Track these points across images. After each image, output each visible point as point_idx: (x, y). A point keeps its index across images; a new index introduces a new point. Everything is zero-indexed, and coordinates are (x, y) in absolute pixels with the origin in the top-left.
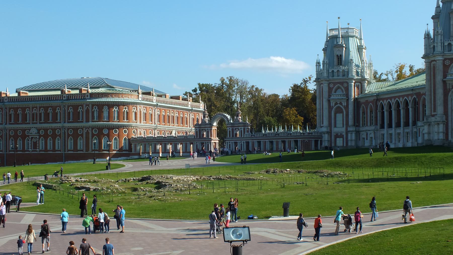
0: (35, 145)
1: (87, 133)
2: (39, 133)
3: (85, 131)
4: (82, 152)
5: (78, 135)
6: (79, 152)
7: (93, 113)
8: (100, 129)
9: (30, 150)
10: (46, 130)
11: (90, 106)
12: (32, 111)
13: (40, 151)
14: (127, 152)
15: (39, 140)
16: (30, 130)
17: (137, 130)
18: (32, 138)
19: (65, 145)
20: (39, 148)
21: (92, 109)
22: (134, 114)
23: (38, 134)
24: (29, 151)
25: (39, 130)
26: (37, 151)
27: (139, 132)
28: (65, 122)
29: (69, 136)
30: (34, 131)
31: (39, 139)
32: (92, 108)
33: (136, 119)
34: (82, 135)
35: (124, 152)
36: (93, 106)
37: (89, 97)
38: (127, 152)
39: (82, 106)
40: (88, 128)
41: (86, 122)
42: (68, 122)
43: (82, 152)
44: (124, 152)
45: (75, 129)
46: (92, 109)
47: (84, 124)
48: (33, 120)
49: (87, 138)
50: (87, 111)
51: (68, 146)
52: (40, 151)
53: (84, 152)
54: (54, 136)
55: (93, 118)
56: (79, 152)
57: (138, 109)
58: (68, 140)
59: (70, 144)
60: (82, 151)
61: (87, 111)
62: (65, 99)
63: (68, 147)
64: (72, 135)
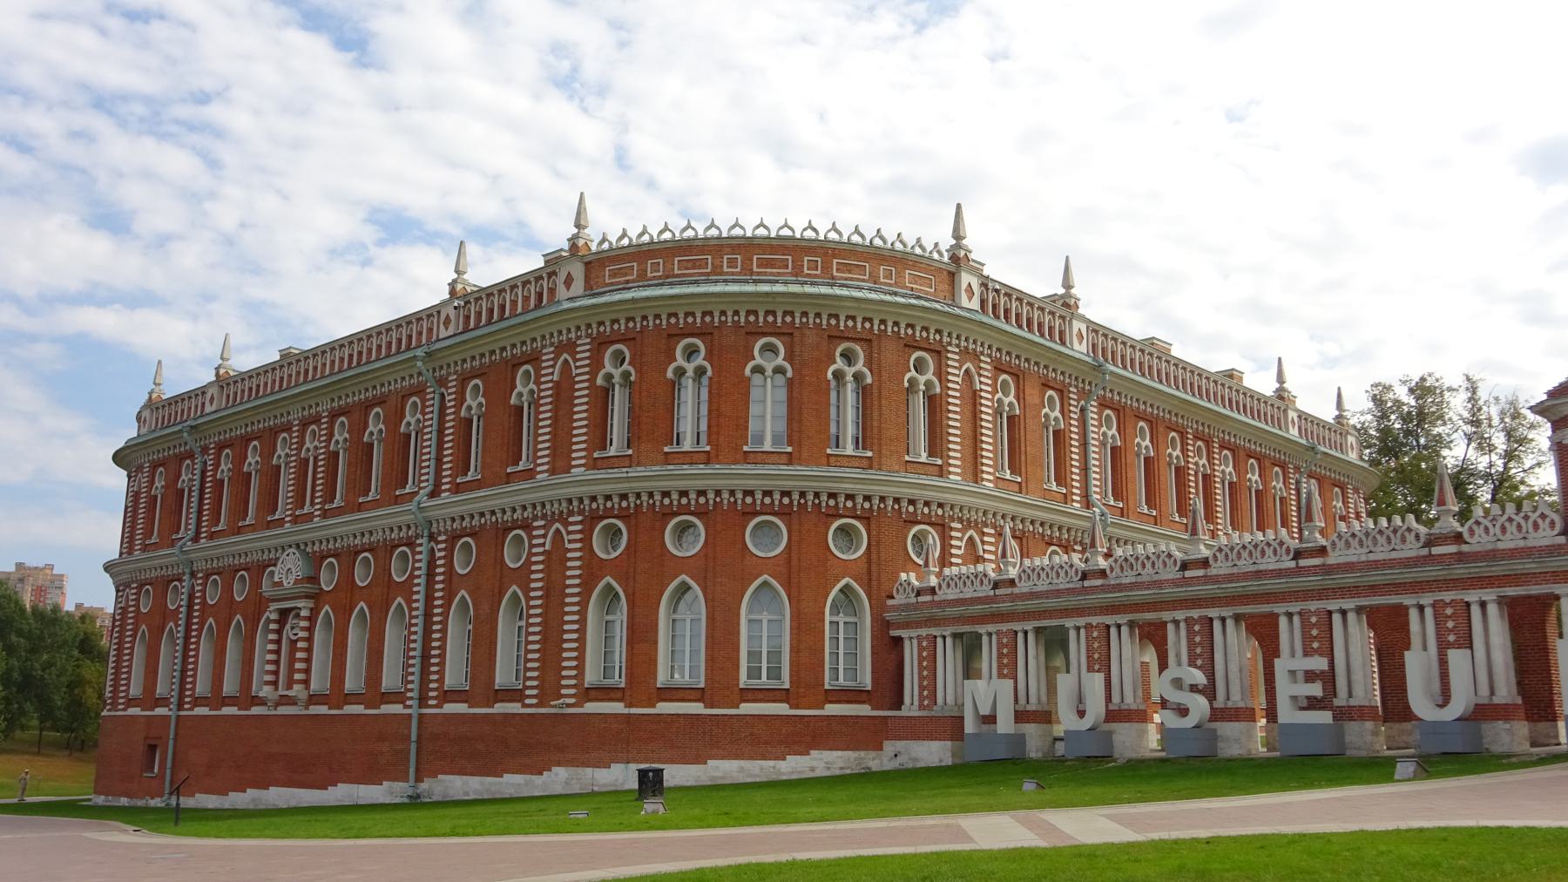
0: (292, 661)
2: (314, 579)
4: (514, 708)
5: (503, 577)
7: (602, 398)
8: (644, 518)
9: (266, 692)
10: (348, 556)
11: (584, 346)
13: (314, 699)
14: (864, 710)
15: (310, 629)
17: (943, 528)
18: (284, 614)
20: (306, 682)
21: (593, 374)
22: (919, 404)
23: (308, 588)
24: (261, 702)
25: (316, 560)
27: (959, 546)
28: (434, 494)
30: (289, 570)
31: (312, 619)
32: (596, 364)
33: (936, 444)
34: (522, 576)
35: (832, 709)
36: (600, 344)
37: (578, 287)
38: (864, 710)
39: (534, 359)
41: (553, 472)
43: (514, 708)
44: (832, 709)
45: (492, 534)
46: (593, 374)
47: (545, 487)
49: (553, 594)
50: (563, 392)
51: (442, 664)
52: (314, 699)
55: (600, 438)
57: (956, 377)
58: (447, 606)
61: (563, 392)
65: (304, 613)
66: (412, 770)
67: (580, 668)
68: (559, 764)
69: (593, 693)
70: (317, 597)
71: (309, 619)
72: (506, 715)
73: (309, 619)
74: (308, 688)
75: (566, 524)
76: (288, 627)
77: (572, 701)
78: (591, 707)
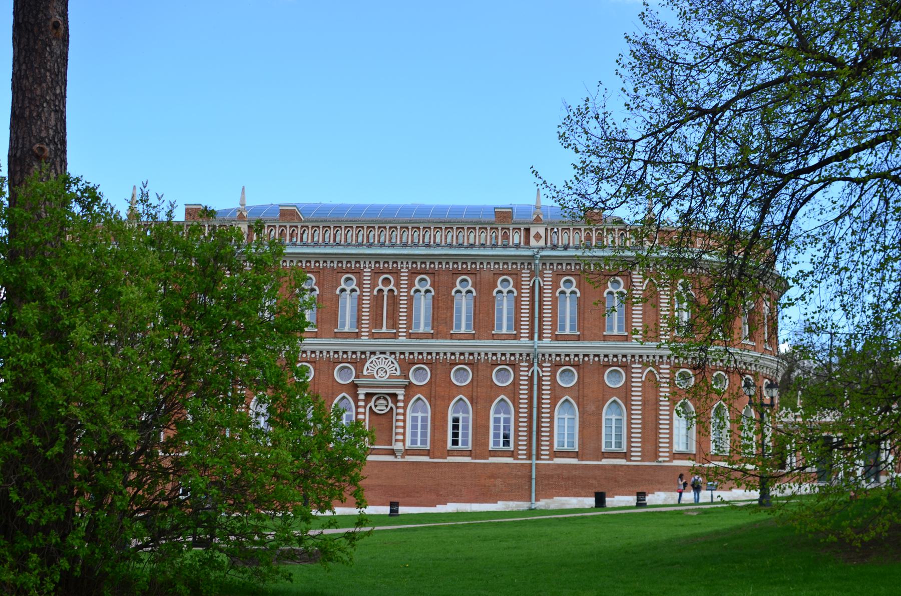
1: (652, 384)
3: (639, 375)
5: (608, 392)
6: (605, 462)
12: (374, 285)
13: (407, 452)
15: (405, 408)
16: (359, 364)
19: (536, 429)
20: (404, 441)
25: (406, 365)
26: (393, 452)
29: (557, 393)
34: (626, 393)
40: (654, 364)
42: (557, 338)
48: (376, 321)
52: (407, 452)
53: (636, 460)
54: (481, 396)
56: (605, 462)
59: (565, 427)
60: (626, 456)
62: (542, 243)
63: (551, 442)
64: (579, 393)
65: (401, 398)
66: (533, 495)
67: (671, 443)
68: (659, 490)
69: (677, 456)
70: (408, 387)
71: (403, 401)
72: (615, 466)
73: (403, 401)
74: (404, 445)
75: (658, 368)
76: (372, 404)
77: (667, 459)
78: (676, 463)
